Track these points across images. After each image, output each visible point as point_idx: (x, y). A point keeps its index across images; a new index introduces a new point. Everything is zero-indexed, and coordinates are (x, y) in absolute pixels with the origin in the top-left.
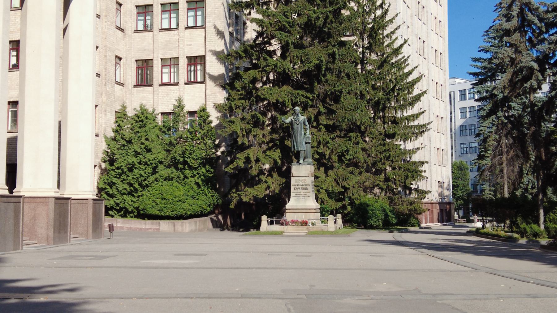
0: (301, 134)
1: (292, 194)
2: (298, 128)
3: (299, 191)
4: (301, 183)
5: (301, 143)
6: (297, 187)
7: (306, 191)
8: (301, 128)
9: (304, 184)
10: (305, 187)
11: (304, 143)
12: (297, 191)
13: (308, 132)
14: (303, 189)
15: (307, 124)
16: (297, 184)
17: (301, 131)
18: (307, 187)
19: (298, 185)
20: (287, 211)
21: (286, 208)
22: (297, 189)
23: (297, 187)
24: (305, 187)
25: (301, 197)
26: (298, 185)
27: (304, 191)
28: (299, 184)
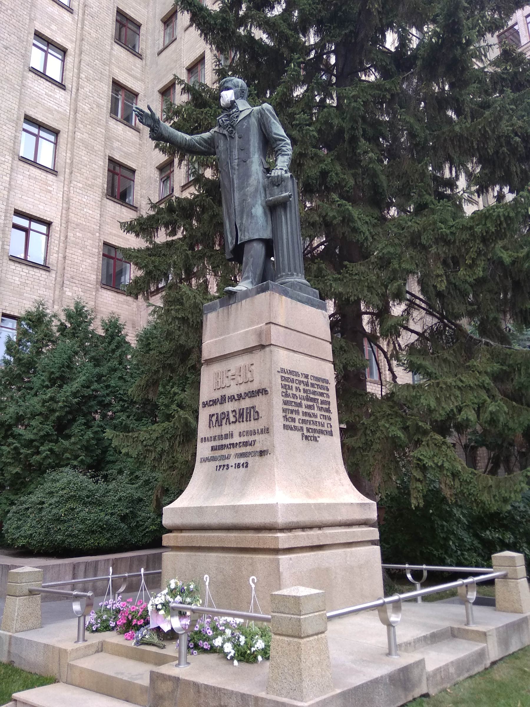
0: (246, 175)
1: (203, 450)
2: (229, 151)
3: (226, 429)
4: (234, 390)
5: (245, 210)
6: (217, 409)
7: (252, 425)
8: (244, 149)
9: (243, 389)
10: (246, 403)
11: (258, 211)
12: (216, 431)
13: (283, 163)
14: (241, 416)
15: (278, 129)
16: (217, 395)
17: (244, 161)
18: (258, 402)
19: (223, 400)
20: (167, 539)
21: (167, 521)
22: (219, 420)
23: (217, 409)
24: (246, 403)
25: (232, 461)
26: (223, 400)
27: (243, 426)
28: (228, 392)
